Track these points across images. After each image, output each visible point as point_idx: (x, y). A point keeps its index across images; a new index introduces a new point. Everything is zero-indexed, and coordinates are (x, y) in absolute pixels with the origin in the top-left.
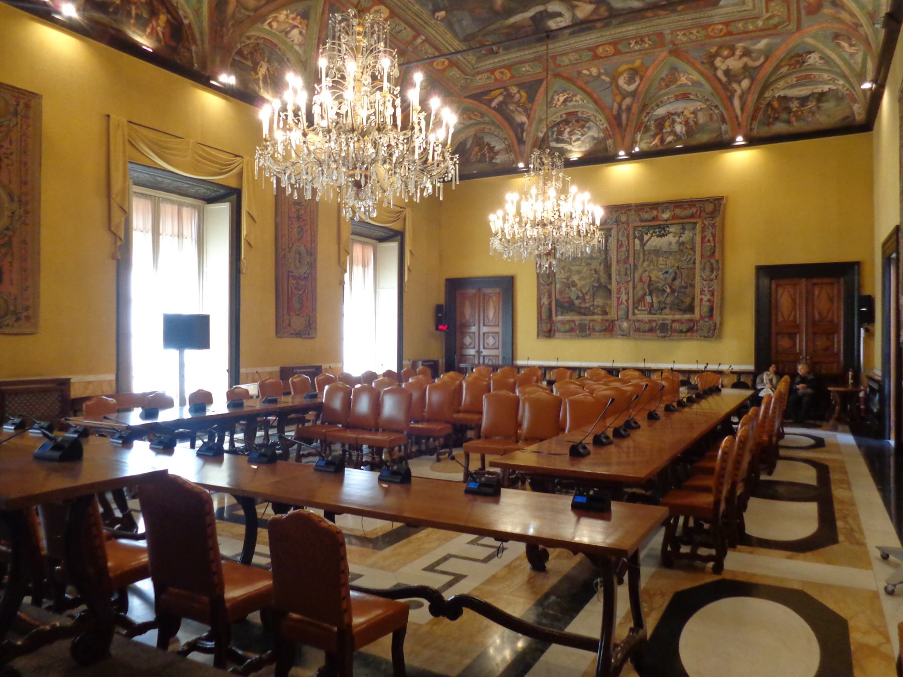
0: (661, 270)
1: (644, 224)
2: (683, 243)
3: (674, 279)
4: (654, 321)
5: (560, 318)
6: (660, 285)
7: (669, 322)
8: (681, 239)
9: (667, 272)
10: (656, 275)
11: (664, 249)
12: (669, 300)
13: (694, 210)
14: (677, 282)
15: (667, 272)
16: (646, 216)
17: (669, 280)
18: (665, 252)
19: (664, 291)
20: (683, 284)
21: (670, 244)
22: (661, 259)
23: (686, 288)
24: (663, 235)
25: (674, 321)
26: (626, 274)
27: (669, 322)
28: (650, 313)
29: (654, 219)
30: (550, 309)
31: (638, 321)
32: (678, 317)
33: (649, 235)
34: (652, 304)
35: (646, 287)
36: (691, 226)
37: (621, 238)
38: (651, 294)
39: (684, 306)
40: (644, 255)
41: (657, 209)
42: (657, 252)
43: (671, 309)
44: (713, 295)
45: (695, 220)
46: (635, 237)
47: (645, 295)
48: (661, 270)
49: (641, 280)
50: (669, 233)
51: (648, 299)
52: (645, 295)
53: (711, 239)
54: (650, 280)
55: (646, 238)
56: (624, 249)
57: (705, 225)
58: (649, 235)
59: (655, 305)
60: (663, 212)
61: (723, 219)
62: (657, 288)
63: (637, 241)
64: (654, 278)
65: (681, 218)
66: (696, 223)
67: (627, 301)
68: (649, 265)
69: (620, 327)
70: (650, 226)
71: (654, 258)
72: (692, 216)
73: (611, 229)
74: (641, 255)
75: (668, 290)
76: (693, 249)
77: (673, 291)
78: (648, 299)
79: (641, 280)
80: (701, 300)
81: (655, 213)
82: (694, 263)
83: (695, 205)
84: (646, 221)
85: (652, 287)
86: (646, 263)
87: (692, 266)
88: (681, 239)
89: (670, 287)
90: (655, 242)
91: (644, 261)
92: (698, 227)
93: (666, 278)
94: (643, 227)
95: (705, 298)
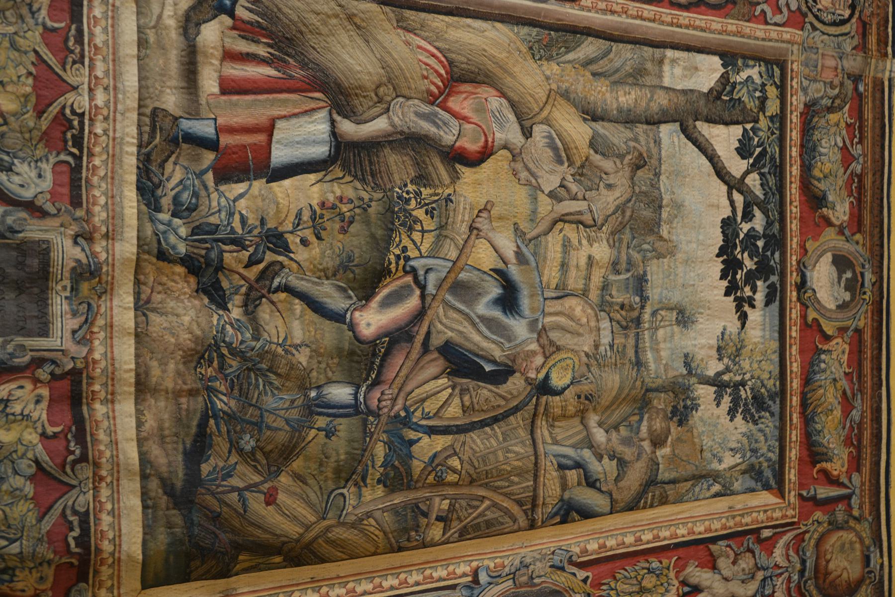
0: (529, 244)
1: (794, 119)
2: (682, 413)
3: (461, 364)
4: (74, 186)
6: (417, 245)
7: (60, 336)
8: (705, 393)
9: (508, 301)
10: (492, 208)
11: (655, 272)
12: (288, 327)
13: (837, 466)
14: (433, 391)
15: (508, 301)
17: (449, 324)
18: (640, 284)
19: (367, 283)
20: (427, 447)
21: (684, 318)
22: (602, 251)
23: (397, 478)
24: (730, 267)
25: (72, 390)
27: (60, 336)
28: (163, 140)
29: (815, 200)
32: (121, 426)
33: (737, 166)
34: (246, 162)
35: (408, 115)
36: (768, 450)
38: (346, 156)
39: (232, 475)
40: (628, 119)
41: (856, 222)
42: (643, 222)
43: (205, 352)
45: (792, 475)
46: (730, 57)
47: (341, 98)
48: (529, 244)
49: (460, 76)
50: (742, 305)
51: (304, 134)
52: (341, 98)
54: (458, 158)
55: (724, 139)
57: (768, 545)
58: (737, 166)
59: (248, 199)
60: (841, 262)
62: (395, 218)
63: (707, 73)
64: (473, 187)
65: (807, 381)
68: (562, 152)
70: (779, 170)
71: (606, 201)
72: (813, 453)
74: (628, 98)
75: (372, 320)
76: (652, 492)
77: (366, 360)
78: (304, 134)
79: (460, 76)
81: (840, 210)
82: (570, 512)
83: (856, 464)
84: (808, 149)
85: (398, 166)
86: (578, 131)
87: (551, 489)
88: (705, 393)
89: (398, 336)
90: (699, 205)
91: (592, 115)
93: (464, 290)
94: (781, 119)
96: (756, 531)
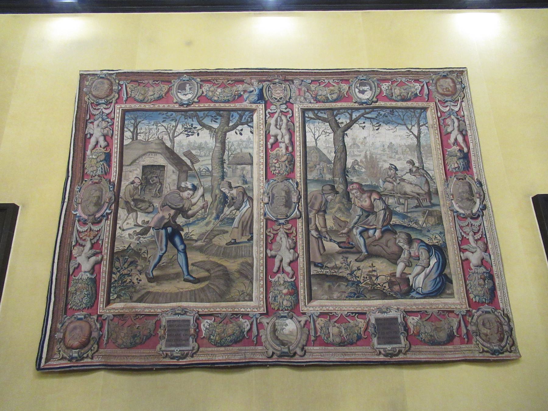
5: (118, 306)
16: (323, 92)
26: (288, 204)
30: (95, 282)
31: (322, 315)
37: (273, 131)
44: (486, 250)
53: (460, 139)
56: (282, 149)
61: (470, 105)
66: (425, 109)
67: (293, 263)
69: (274, 330)
73: (252, 111)
80: (465, 262)
92: (431, 115)
95: (474, 259)
96: (438, 118)
